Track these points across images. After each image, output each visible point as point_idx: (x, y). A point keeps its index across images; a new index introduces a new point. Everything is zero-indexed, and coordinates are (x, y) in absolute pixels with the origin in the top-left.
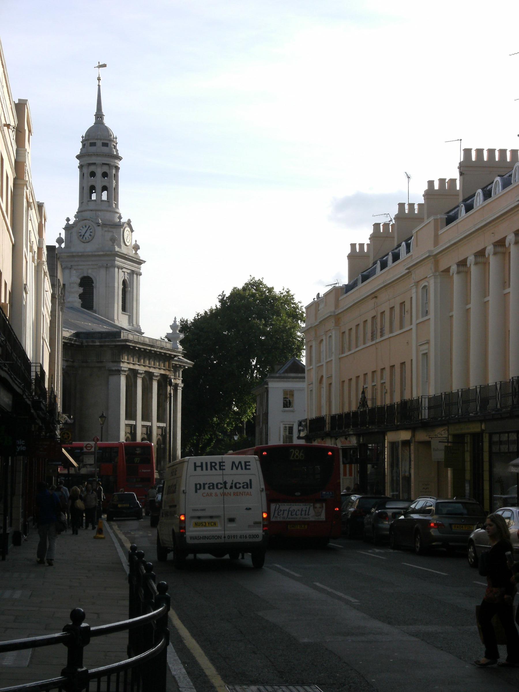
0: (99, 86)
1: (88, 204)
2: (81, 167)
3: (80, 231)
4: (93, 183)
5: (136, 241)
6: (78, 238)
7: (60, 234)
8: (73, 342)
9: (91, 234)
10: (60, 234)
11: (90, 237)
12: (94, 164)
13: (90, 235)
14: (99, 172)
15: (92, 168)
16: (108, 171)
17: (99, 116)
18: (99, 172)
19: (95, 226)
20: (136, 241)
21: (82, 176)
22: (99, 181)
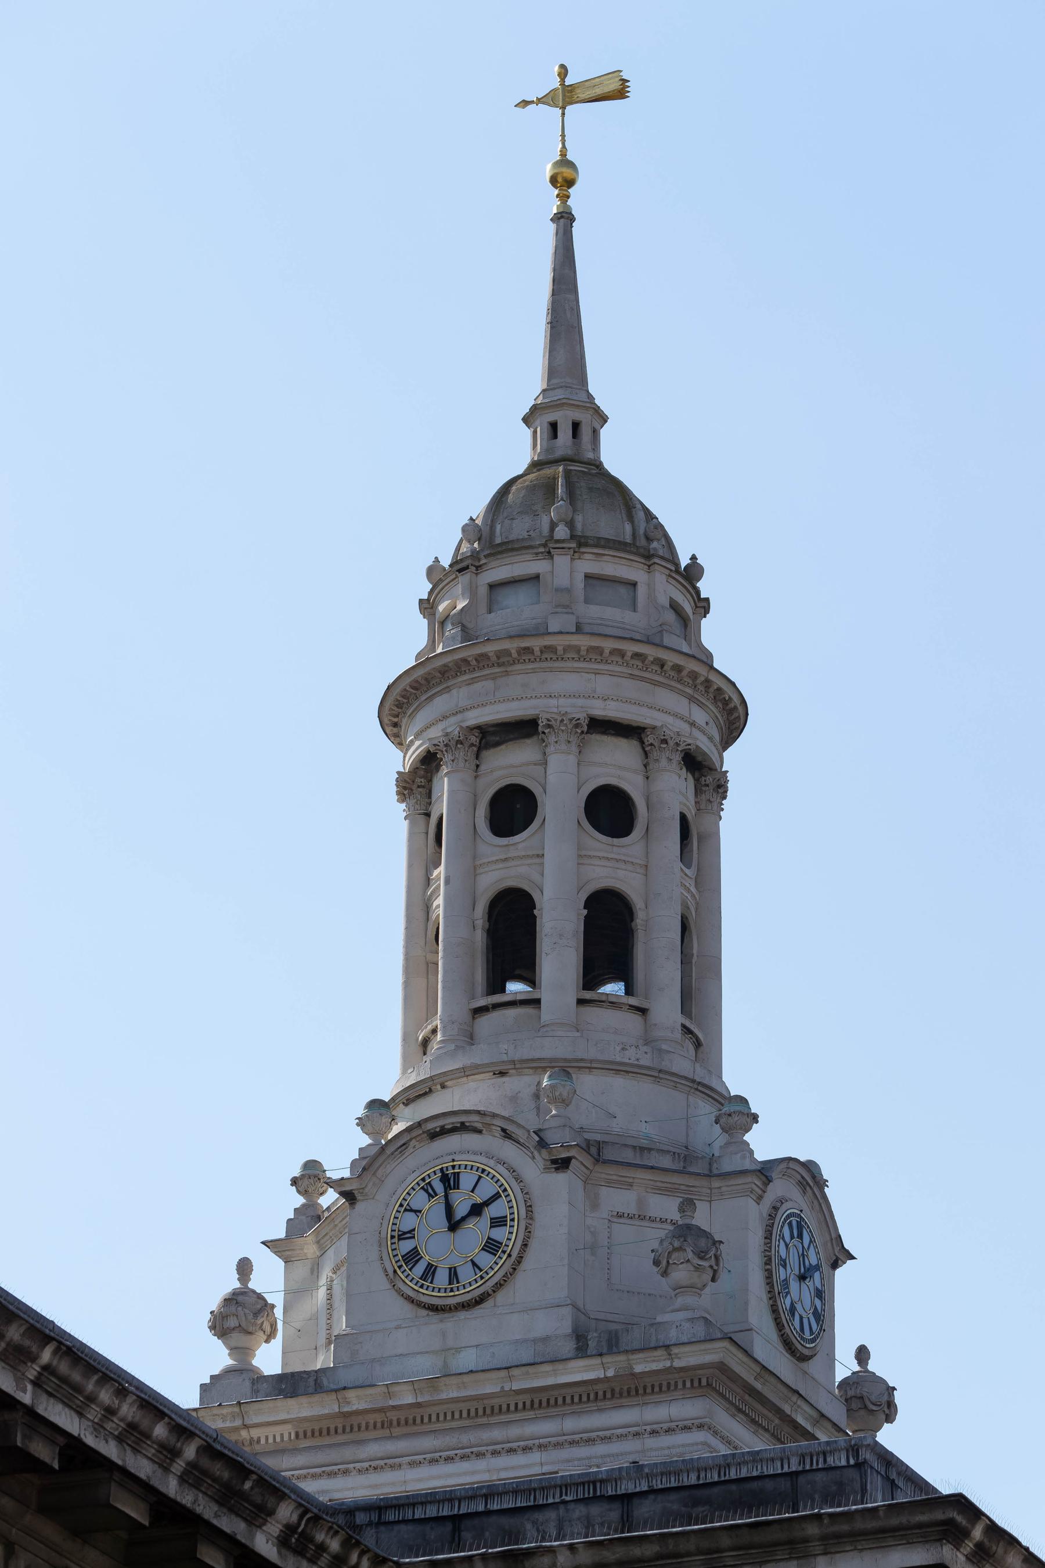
0: (564, 219)
1: (471, 1038)
2: (416, 785)
3: (409, 1221)
4: (513, 876)
5: (862, 1354)
6: (392, 1278)
7: (244, 1268)
8: (264, 1544)
9: (499, 1234)
10: (244, 1268)
11: (486, 1260)
12: (524, 728)
13: (492, 1246)
14: (561, 781)
15: (510, 764)
16: (632, 785)
17: (567, 419)
18: (561, 781)
19: (531, 1168)
20: (862, 1354)
21: (429, 839)
22: (559, 867)
